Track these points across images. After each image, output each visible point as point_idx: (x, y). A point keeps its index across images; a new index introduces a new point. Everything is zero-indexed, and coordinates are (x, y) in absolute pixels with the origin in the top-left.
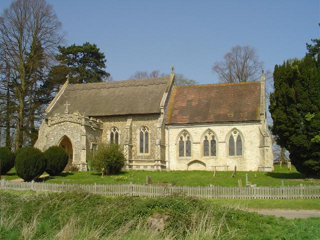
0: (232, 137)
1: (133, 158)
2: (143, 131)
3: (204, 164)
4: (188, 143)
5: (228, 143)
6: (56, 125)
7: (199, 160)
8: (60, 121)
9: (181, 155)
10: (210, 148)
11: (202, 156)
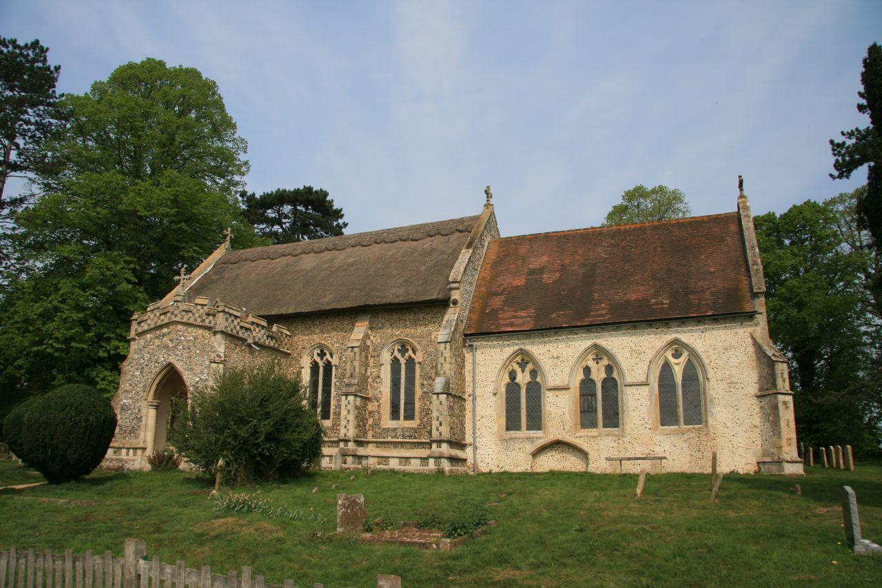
6: (149, 336)
8: (160, 323)
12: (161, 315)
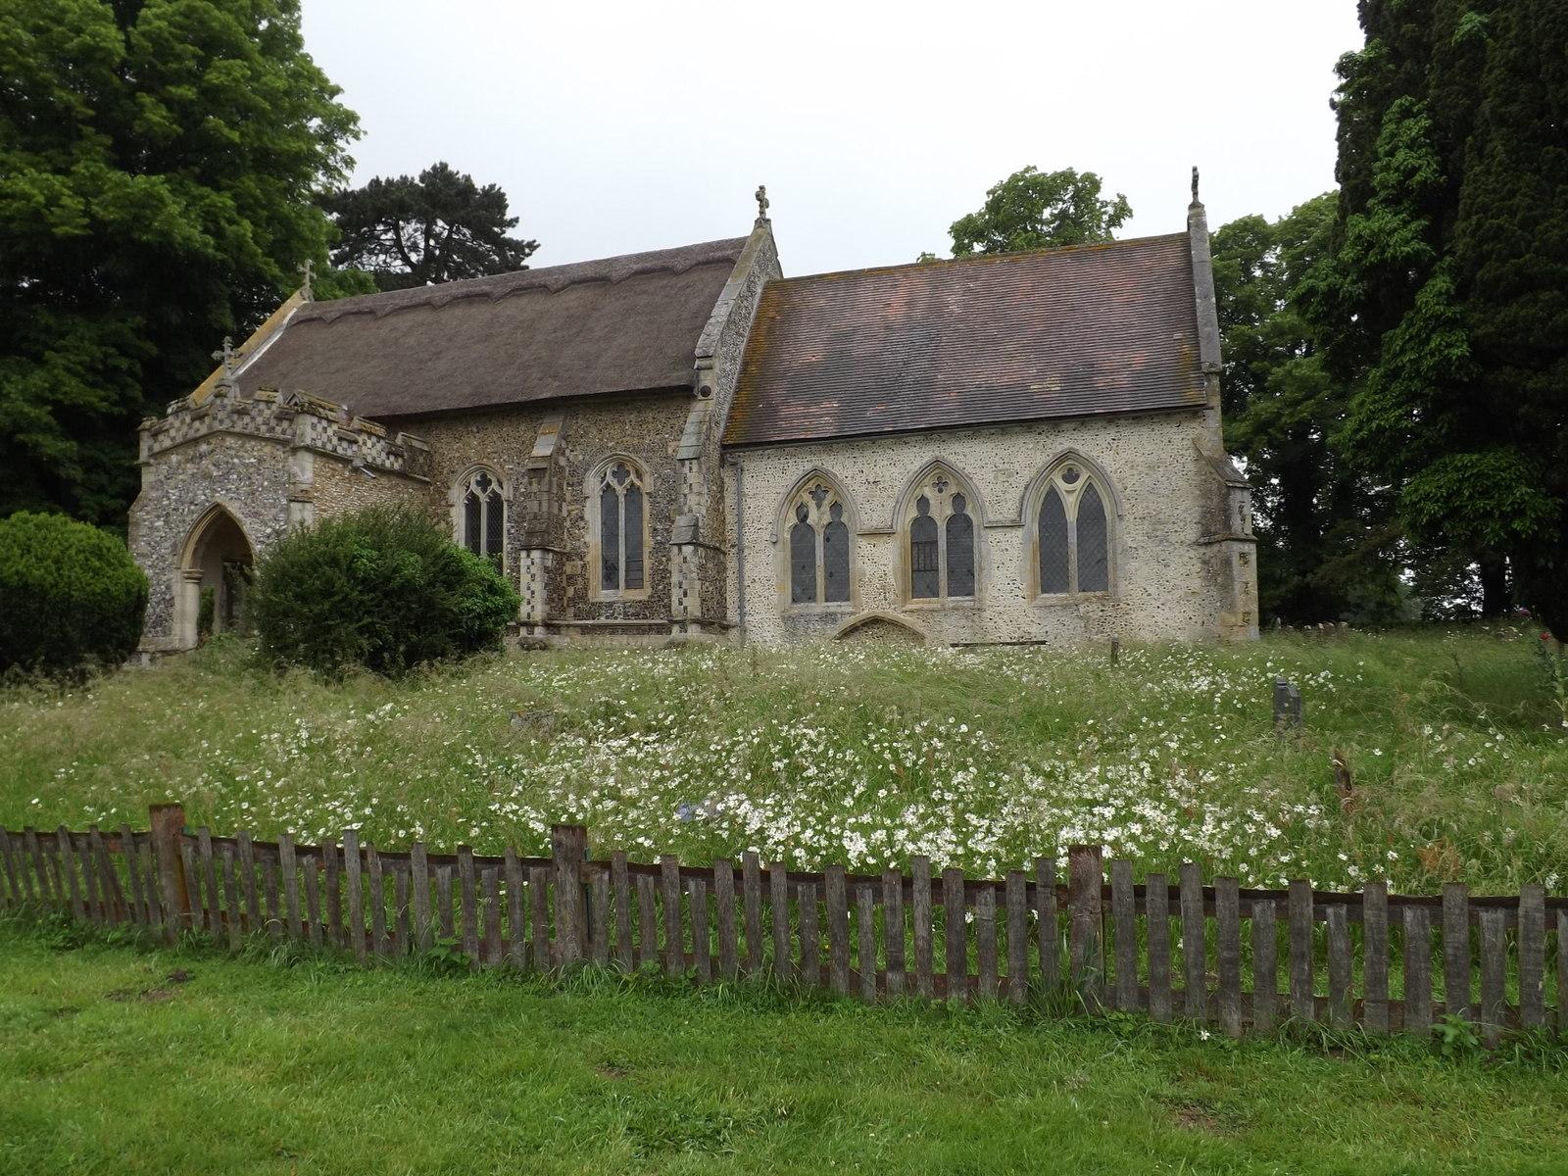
0: (1053, 500)
2: (614, 483)
3: (917, 637)
4: (838, 535)
5: (1036, 528)
6: (174, 458)
7: (892, 613)
8: (192, 434)
9: (802, 591)
10: (942, 557)
11: (904, 592)
12: (193, 420)
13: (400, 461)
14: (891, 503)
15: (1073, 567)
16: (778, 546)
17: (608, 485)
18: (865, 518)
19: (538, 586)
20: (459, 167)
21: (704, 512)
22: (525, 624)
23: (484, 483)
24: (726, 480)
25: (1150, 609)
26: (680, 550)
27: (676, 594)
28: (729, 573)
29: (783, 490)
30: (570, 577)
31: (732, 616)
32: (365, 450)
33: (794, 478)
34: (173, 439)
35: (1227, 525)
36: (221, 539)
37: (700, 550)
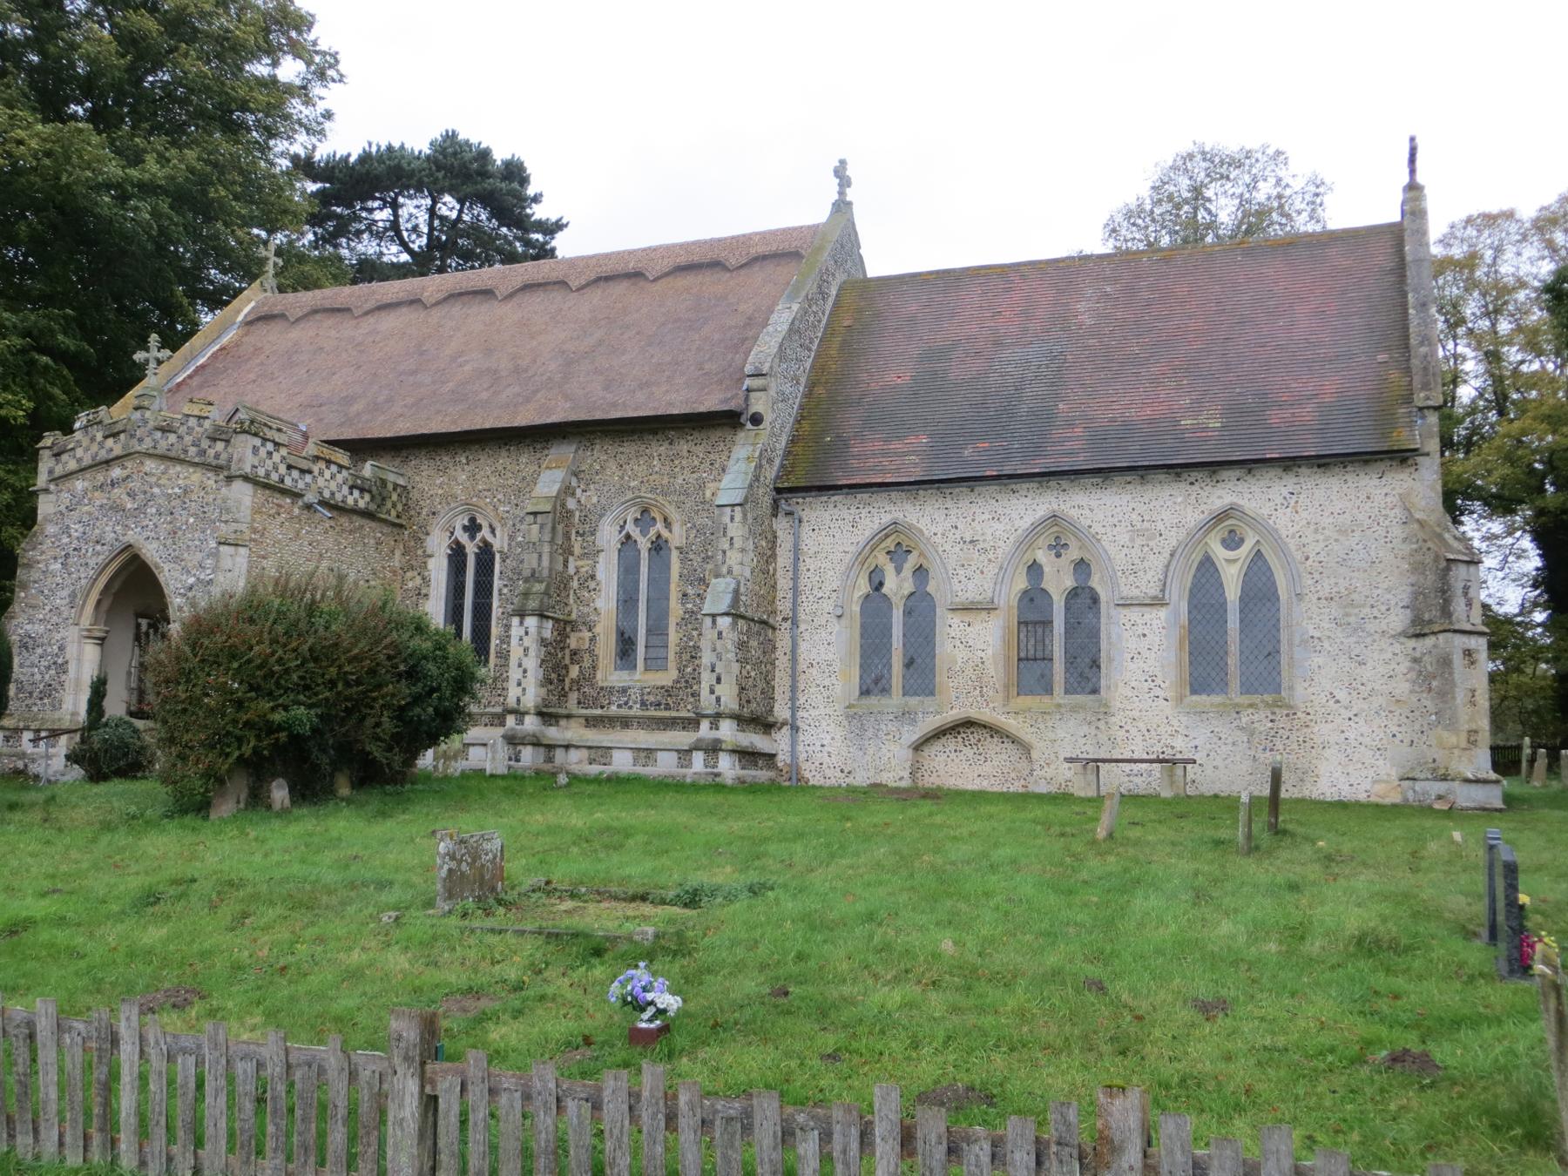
1: (573, 697)
3: (1025, 748)
4: (921, 608)
5: (1184, 607)
6: (79, 485)
8: (103, 455)
9: (873, 685)
11: (1007, 687)
12: (106, 437)
13: (367, 497)
14: (992, 570)
15: (1233, 661)
16: (843, 621)
17: (628, 537)
18: (957, 587)
19: (531, 663)
20: (474, 133)
21: (748, 574)
22: (511, 712)
23: (473, 528)
24: (779, 533)
25: (1338, 720)
26: (714, 622)
27: (707, 679)
28: (779, 653)
29: (852, 549)
30: (574, 653)
31: (781, 711)
32: (321, 482)
33: (868, 534)
34: (79, 460)
35: (1446, 612)
36: (133, 590)
37: (741, 622)
